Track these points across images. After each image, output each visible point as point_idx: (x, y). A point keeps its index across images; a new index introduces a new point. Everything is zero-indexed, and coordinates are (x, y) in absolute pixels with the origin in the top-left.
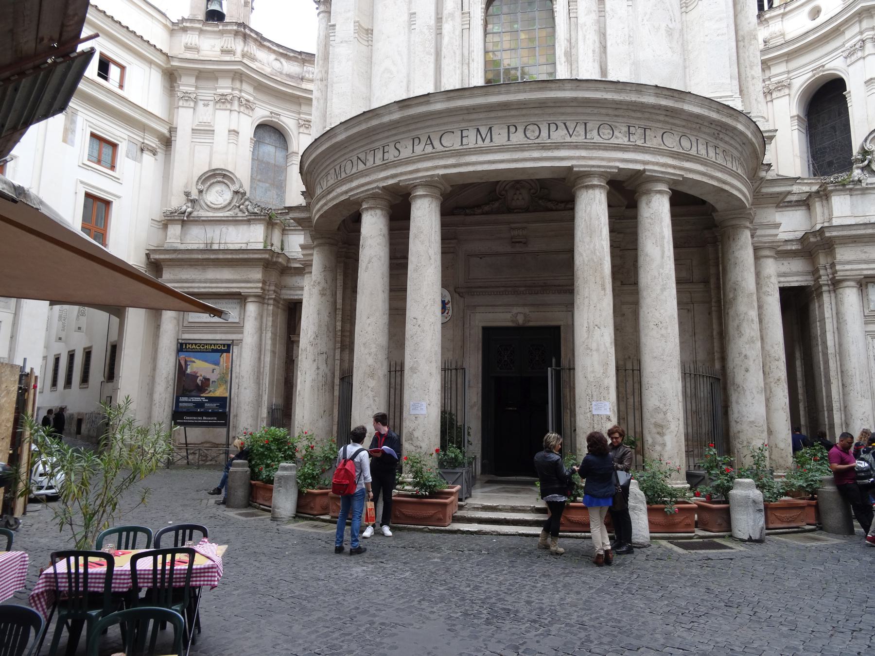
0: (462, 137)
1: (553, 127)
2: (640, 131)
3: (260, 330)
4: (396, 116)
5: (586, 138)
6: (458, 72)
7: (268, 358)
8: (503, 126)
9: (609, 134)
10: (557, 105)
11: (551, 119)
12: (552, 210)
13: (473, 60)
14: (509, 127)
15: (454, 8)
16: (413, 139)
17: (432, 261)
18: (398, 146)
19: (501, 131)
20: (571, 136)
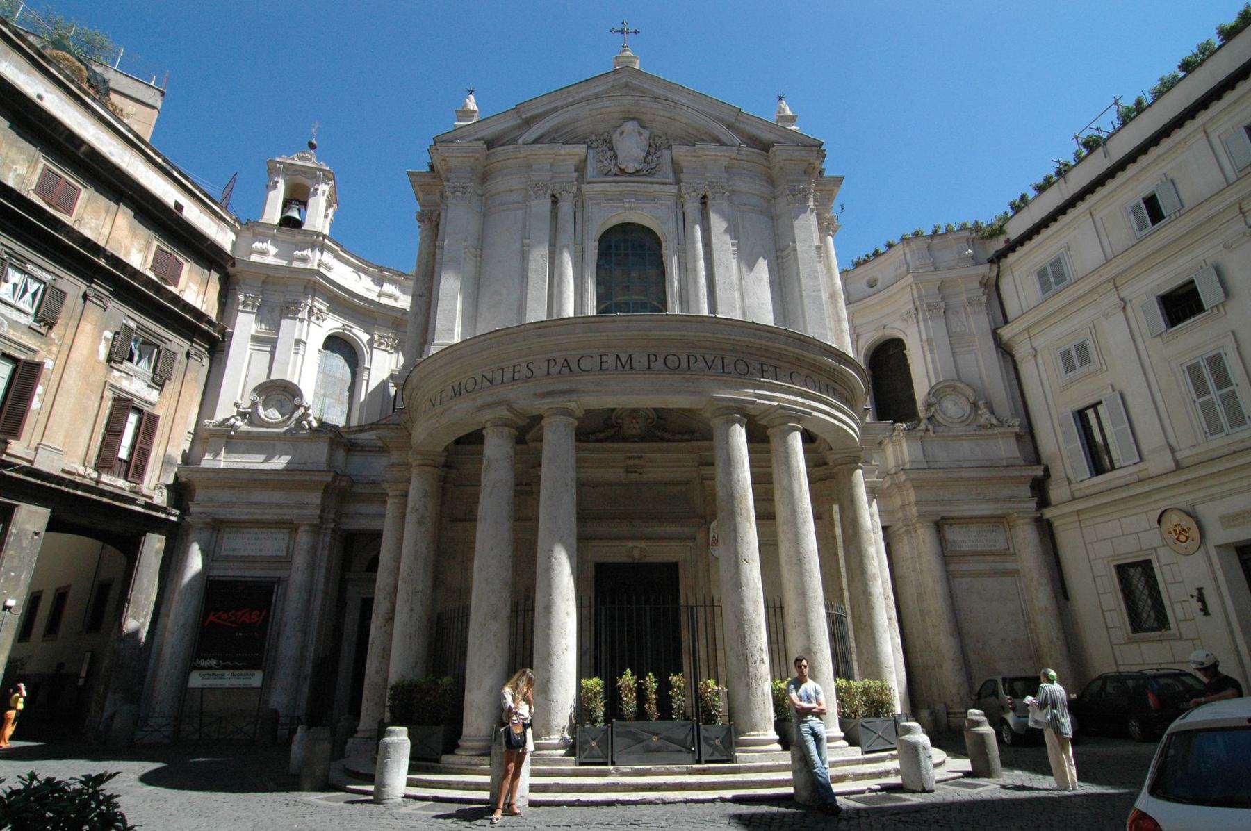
0: (601, 362)
1: (692, 360)
2: (771, 369)
3: (312, 566)
5: (724, 372)
7: (318, 602)
12: (668, 441)
14: (649, 356)
16: (548, 361)
18: (530, 366)
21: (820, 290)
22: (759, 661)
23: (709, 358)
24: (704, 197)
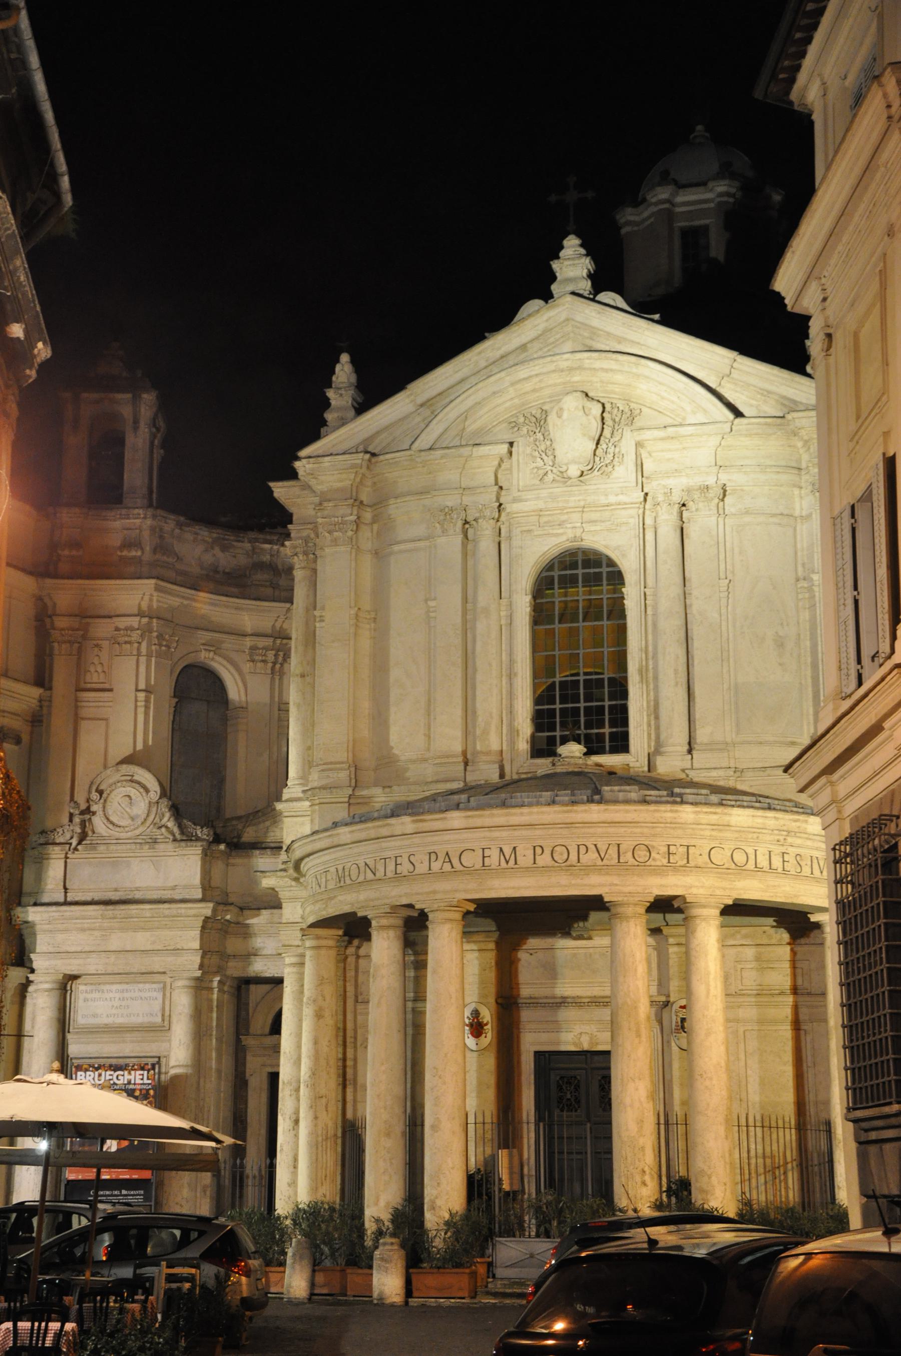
0: (484, 857)
18: (412, 858)
20: (602, 860)
22: (639, 1183)
23: (602, 847)
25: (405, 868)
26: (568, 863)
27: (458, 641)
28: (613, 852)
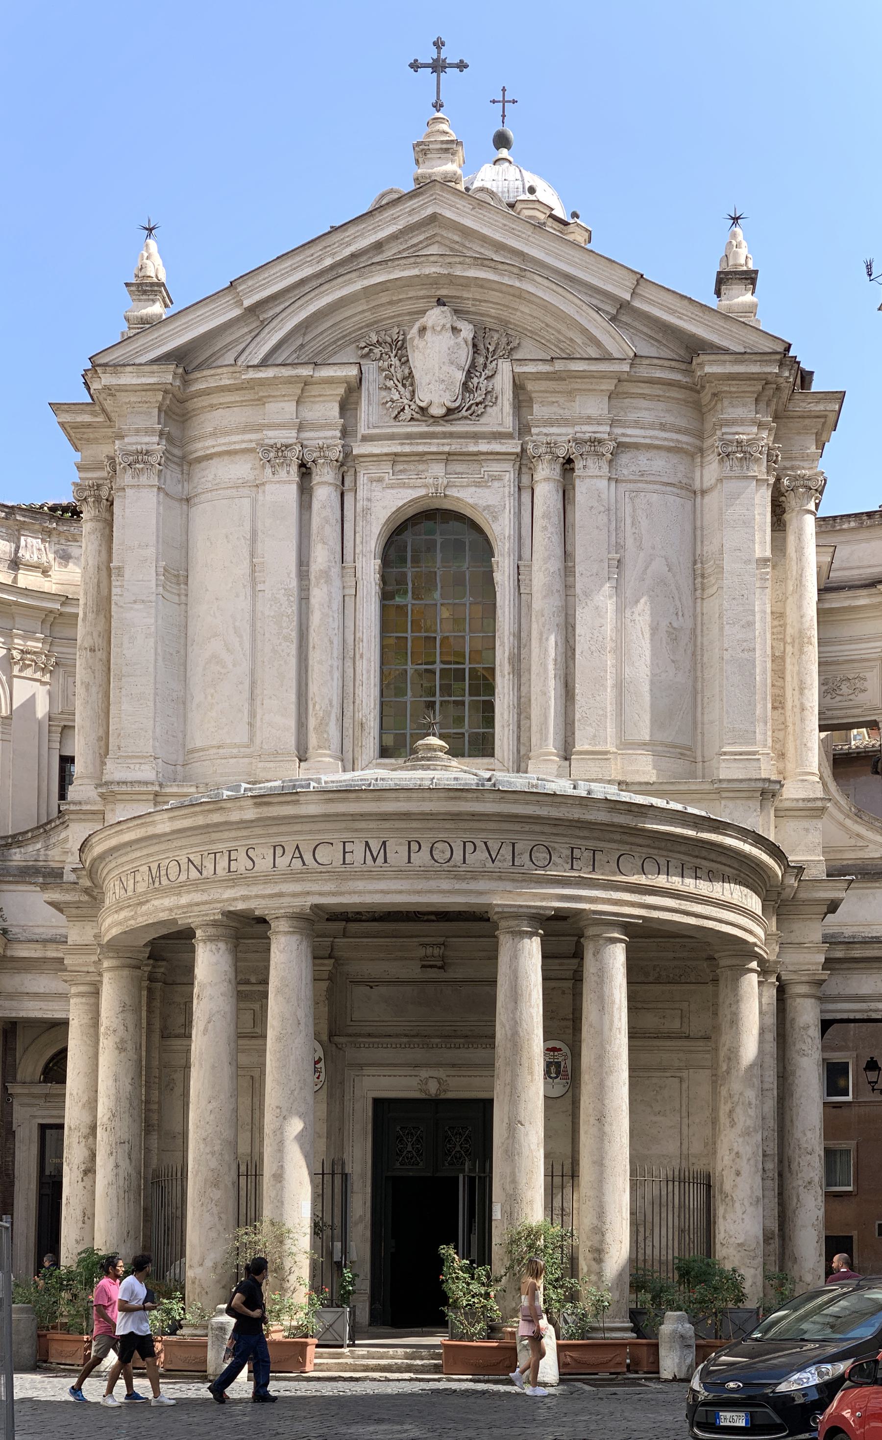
0: (345, 852)
1: (470, 847)
4: (251, 814)
5: (513, 865)
6: (337, 675)
8: (401, 840)
9: (545, 859)
10: (474, 818)
11: (467, 836)
13: (362, 656)
14: (409, 842)
15: (329, 561)
16: (275, 847)
17: (302, 1027)
19: (398, 848)
20: (493, 861)
21: (754, 649)
23: (494, 846)
24: (570, 461)
25: (242, 864)
26: (451, 863)
27: (292, 610)
28: (506, 851)
